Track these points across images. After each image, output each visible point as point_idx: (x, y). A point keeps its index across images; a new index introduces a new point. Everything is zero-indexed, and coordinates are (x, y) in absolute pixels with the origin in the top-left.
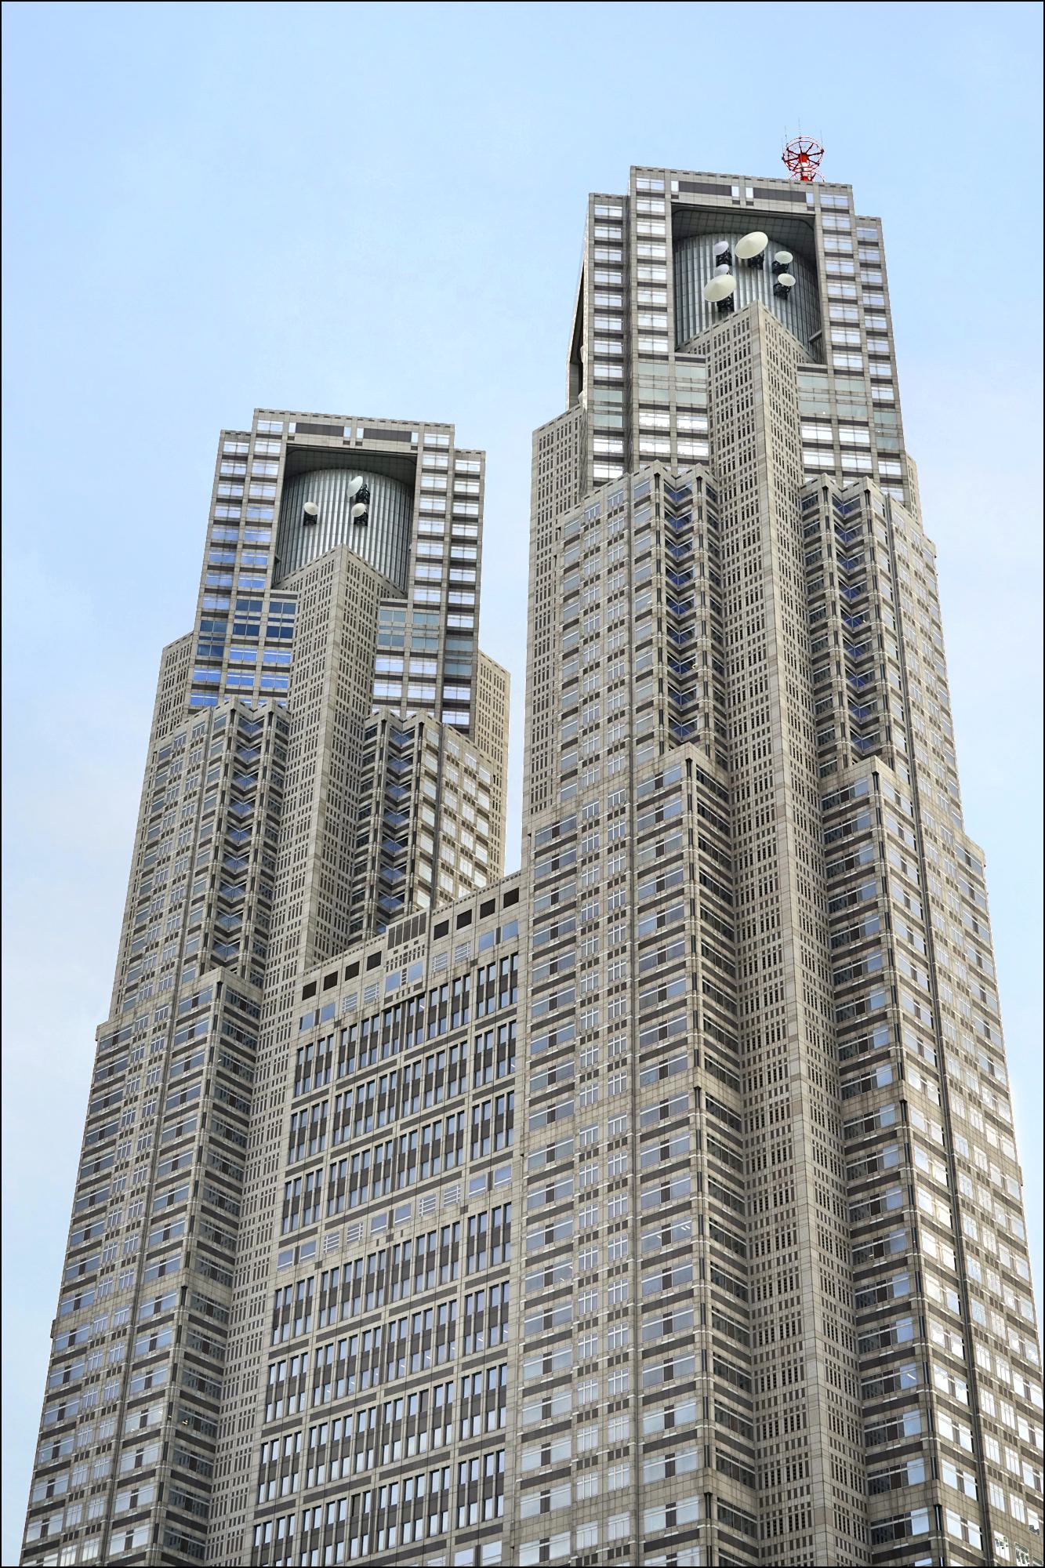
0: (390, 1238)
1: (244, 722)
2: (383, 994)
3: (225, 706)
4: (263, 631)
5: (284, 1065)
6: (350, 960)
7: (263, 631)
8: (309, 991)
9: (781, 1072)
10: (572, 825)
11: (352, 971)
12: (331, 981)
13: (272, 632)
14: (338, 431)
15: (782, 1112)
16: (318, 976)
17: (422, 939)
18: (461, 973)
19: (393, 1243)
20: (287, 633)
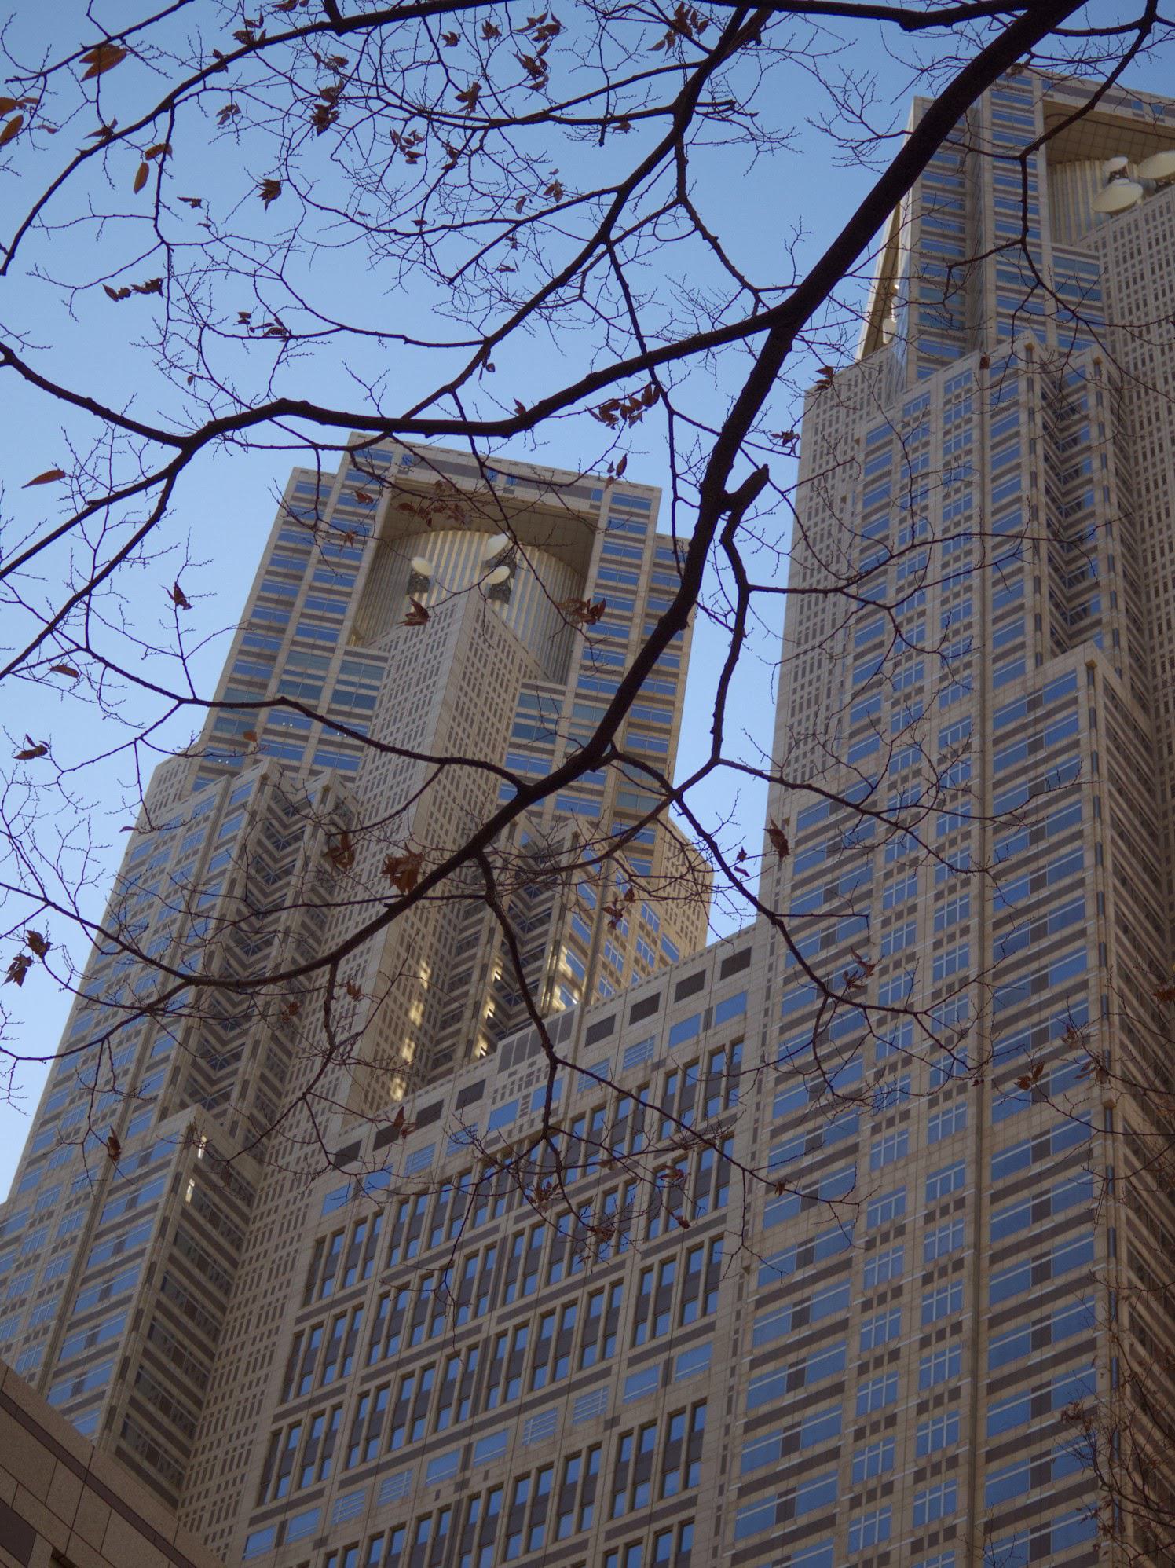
0: (462, 1485)
1: (279, 795)
3: (250, 775)
5: (290, 1264)
19: (466, 1493)
20: (369, 702)
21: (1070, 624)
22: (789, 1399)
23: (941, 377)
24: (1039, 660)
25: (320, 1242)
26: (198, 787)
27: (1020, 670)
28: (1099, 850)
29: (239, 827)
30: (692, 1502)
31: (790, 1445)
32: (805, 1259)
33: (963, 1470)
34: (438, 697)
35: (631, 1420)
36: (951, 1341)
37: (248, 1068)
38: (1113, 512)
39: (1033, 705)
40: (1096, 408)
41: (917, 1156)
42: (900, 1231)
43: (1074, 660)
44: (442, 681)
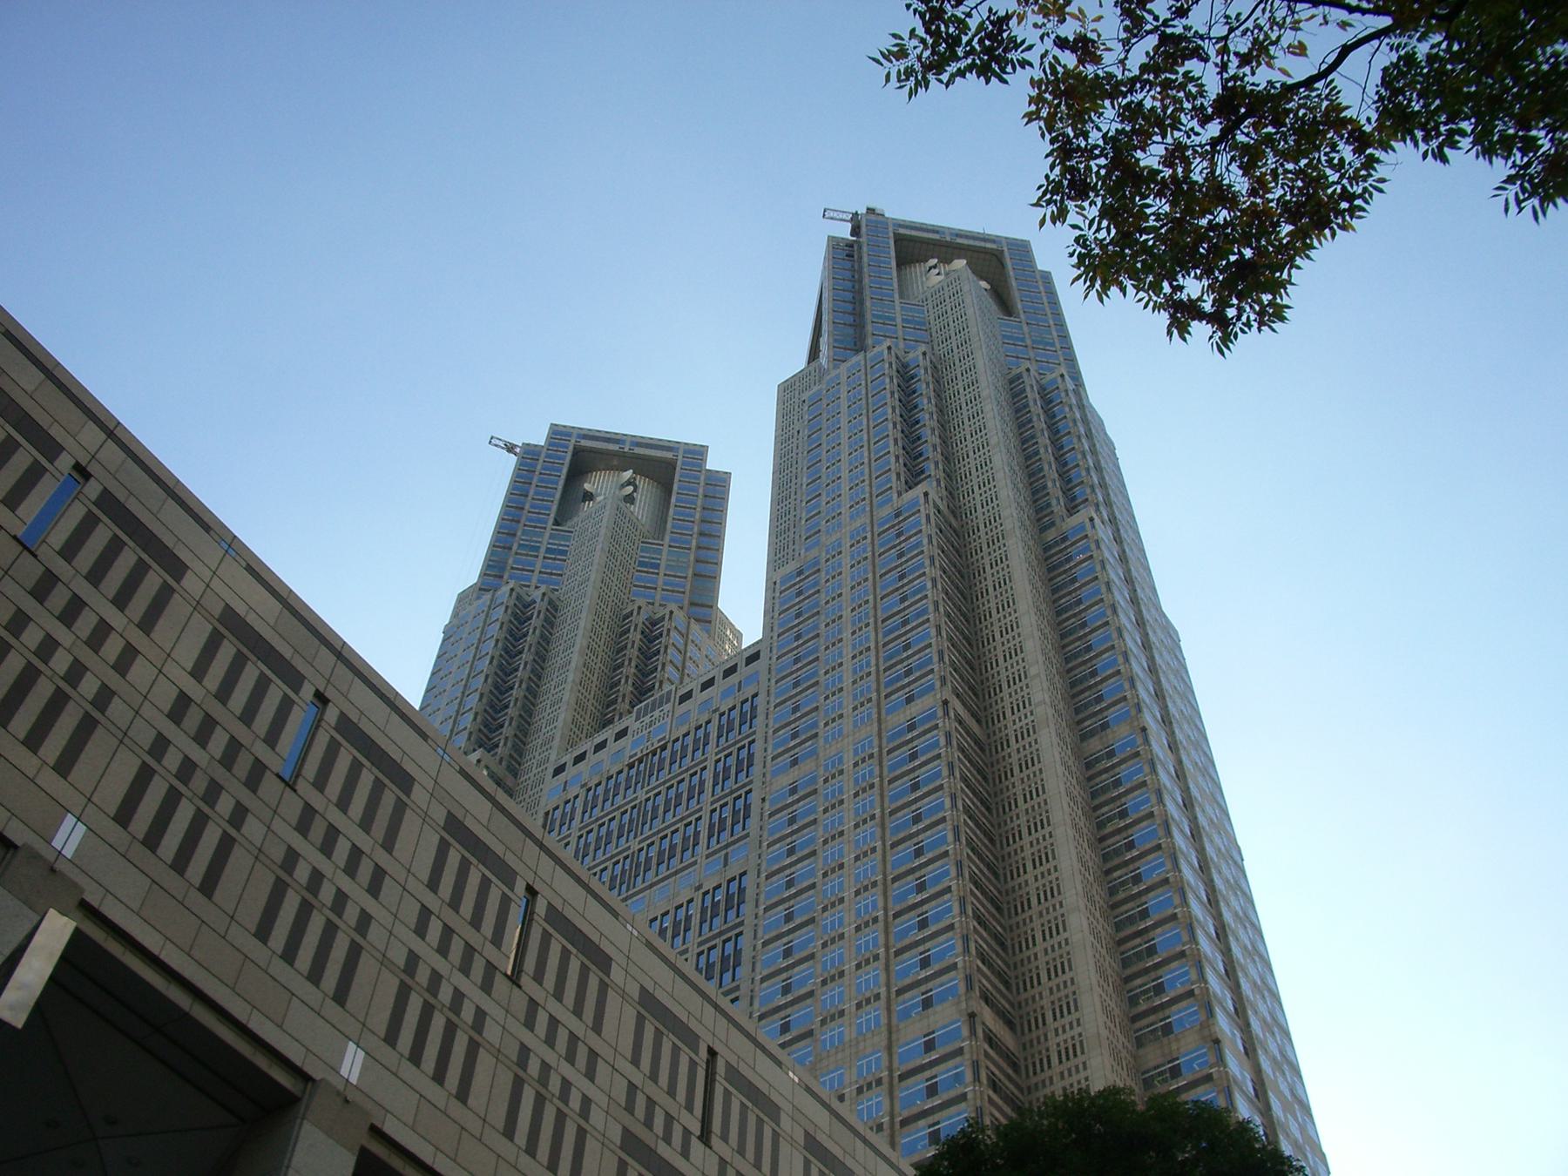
1: (519, 598)
2: (628, 753)
3: (505, 589)
4: (543, 550)
6: (598, 739)
7: (543, 550)
8: (559, 770)
9: (1025, 703)
10: (817, 563)
11: (601, 746)
12: (580, 758)
13: (548, 550)
14: (616, 441)
15: (1031, 730)
16: (568, 758)
17: (667, 707)
18: (702, 722)
21: (914, 476)
22: (788, 861)
23: (844, 367)
24: (900, 494)
25: (547, 814)
26: (478, 598)
27: (890, 500)
28: (934, 581)
29: (499, 613)
30: (741, 924)
31: (790, 884)
32: (793, 791)
33: (880, 887)
34: (599, 547)
35: (708, 886)
36: (870, 823)
37: (508, 731)
38: (934, 424)
39: (897, 516)
40: (924, 388)
41: (847, 740)
42: (841, 772)
43: (918, 491)
44: (601, 539)
